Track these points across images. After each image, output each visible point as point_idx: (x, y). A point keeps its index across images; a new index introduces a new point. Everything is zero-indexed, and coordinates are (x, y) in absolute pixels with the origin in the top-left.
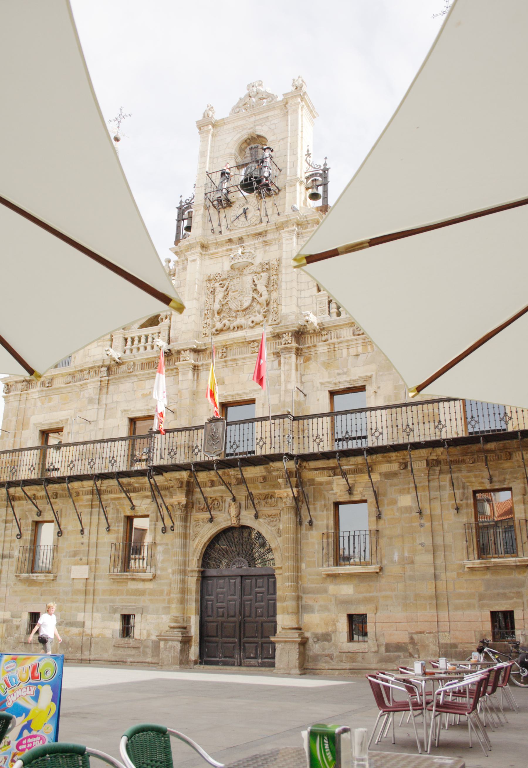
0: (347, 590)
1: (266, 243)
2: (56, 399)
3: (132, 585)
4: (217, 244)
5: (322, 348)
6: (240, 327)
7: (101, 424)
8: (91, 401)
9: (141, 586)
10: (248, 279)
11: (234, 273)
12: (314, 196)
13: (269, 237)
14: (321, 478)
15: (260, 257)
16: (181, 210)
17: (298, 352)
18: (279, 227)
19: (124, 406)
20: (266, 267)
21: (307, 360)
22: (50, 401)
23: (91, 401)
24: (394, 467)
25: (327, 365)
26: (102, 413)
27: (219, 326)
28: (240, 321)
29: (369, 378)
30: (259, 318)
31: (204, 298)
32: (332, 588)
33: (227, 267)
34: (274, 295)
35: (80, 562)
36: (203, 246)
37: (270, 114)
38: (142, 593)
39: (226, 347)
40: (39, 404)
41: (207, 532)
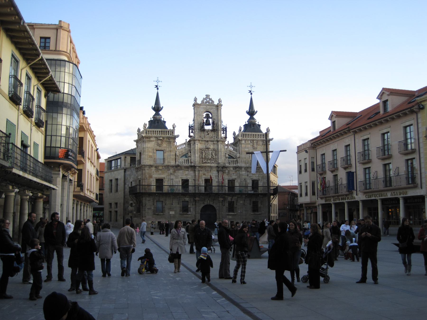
0: (230, 217)
1: (214, 144)
2: (160, 172)
3: (185, 216)
4: (202, 141)
5: (227, 171)
6: (209, 163)
7: (175, 180)
8: (171, 174)
9: (187, 216)
10: (210, 152)
11: (207, 149)
12: (223, 133)
13: (215, 142)
14: (226, 197)
15: (212, 147)
16: (189, 126)
17: (222, 171)
18: (218, 141)
19: (180, 176)
20: (214, 150)
21: (224, 173)
22: (158, 172)
23: (171, 174)
24: (239, 196)
25: (227, 175)
26: (175, 177)
27: (204, 161)
28: (209, 161)
29: (236, 179)
30: (213, 162)
31: (199, 154)
32: (228, 217)
33: (204, 147)
34: (216, 157)
35: (172, 211)
36: (199, 140)
37: (213, 107)
38: (188, 217)
39: (205, 167)
40: (155, 172)
41: (202, 205)
